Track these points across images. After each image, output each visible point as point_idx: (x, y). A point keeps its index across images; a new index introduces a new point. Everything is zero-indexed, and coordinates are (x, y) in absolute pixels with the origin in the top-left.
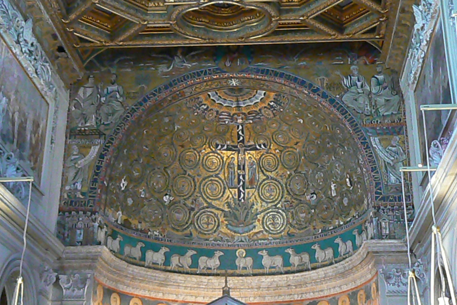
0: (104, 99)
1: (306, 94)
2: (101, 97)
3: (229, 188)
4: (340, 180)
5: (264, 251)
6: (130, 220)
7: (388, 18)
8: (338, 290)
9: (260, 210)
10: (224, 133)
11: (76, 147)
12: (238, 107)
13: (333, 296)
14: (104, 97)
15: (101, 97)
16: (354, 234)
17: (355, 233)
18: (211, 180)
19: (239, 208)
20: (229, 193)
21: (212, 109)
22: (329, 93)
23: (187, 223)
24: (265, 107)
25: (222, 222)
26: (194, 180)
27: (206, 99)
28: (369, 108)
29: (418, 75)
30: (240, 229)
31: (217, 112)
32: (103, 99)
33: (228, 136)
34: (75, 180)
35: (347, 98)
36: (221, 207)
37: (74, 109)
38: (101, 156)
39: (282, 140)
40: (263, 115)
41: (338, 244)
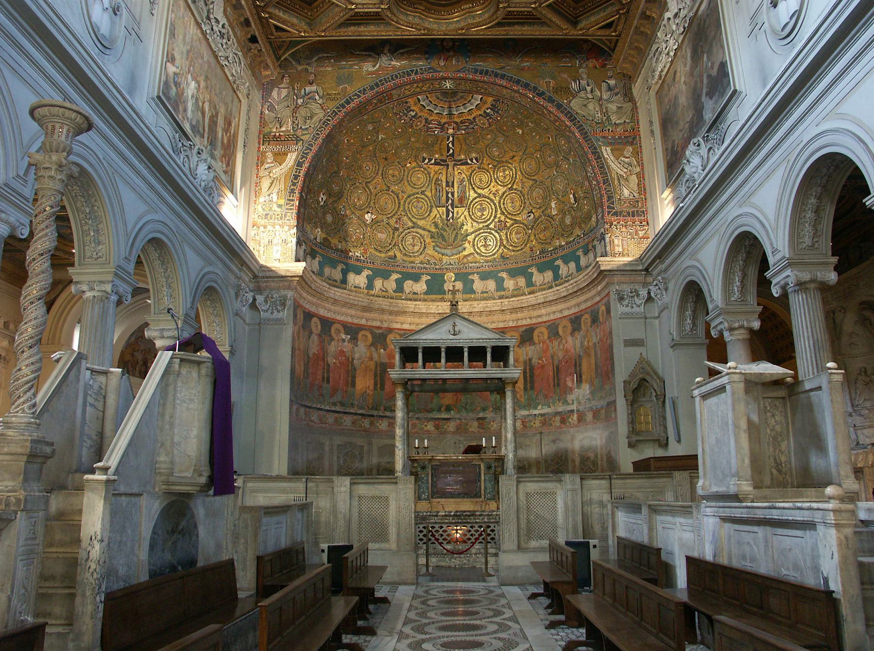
0: (302, 100)
1: (529, 98)
2: (297, 98)
3: (436, 207)
4: (563, 196)
5: (475, 275)
6: (330, 239)
7: (628, 12)
8: (559, 315)
9: (470, 230)
10: (433, 145)
11: (269, 155)
12: (450, 114)
13: (553, 322)
14: (301, 98)
15: (297, 98)
16: (578, 253)
17: (580, 253)
18: (417, 198)
19: (447, 229)
20: (436, 212)
21: (421, 117)
22: (556, 97)
23: (390, 244)
24: (480, 115)
25: (429, 243)
26: (398, 197)
27: (415, 104)
28: (599, 115)
29: (664, 73)
30: (448, 252)
31: (427, 119)
32: (300, 101)
33: (436, 148)
34: (270, 191)
35: (575, 104)
36: (428, 227)
37: (267, 112)
38: (299, 164)
39: (497, 153)
40: (477, 125)
41: (558, 266)
